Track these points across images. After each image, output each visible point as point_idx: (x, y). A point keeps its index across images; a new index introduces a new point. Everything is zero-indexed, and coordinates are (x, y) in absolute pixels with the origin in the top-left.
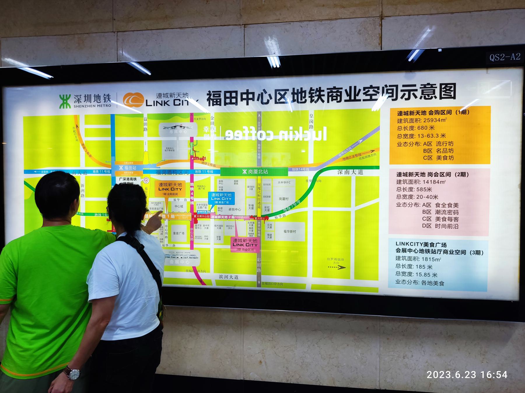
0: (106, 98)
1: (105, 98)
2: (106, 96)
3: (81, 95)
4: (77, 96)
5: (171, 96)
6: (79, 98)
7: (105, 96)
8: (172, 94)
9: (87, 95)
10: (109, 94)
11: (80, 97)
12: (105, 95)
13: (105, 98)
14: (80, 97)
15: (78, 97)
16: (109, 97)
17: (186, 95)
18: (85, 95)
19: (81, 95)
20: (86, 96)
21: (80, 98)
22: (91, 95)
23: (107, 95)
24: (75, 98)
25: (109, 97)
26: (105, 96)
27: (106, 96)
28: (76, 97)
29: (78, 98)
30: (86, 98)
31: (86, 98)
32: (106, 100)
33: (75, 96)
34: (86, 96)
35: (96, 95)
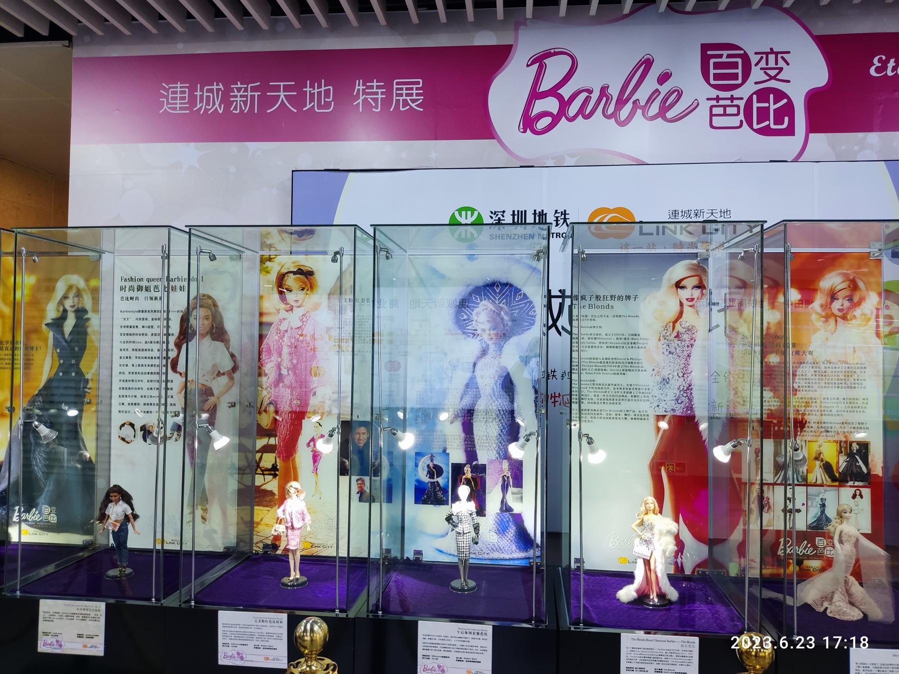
0: (559, 219)
1: (557, 217)
2: (560, 215)
3: (504, 212)
4: (495, 212)
5: (696, 215)
6: (499, 218)
7: (557, 215)
8: (699, 212)
9: (518, 211)
10: (565, 211)
11: (503, 216)
12: (556, 212)
13: (557, 217)
14: (503, 216)
15: (497, 215)
16: (565, 217)
17: (726, 213)
18: (514, 211)
19: (504, 212)
20: (516, 213)
21: (502, 218)
22: (525, 211)
23: (562, 212)
24: (492, 218)
25: (565, 217)
26: (557, 215)
27: (560, 215)
28: (492, 215)
29: (497, 218)
30: (516, 217)
31: (516, 217)
32: (559, 222)
33: (492, 213)
34: (516, 213)
35: (537, 212)
